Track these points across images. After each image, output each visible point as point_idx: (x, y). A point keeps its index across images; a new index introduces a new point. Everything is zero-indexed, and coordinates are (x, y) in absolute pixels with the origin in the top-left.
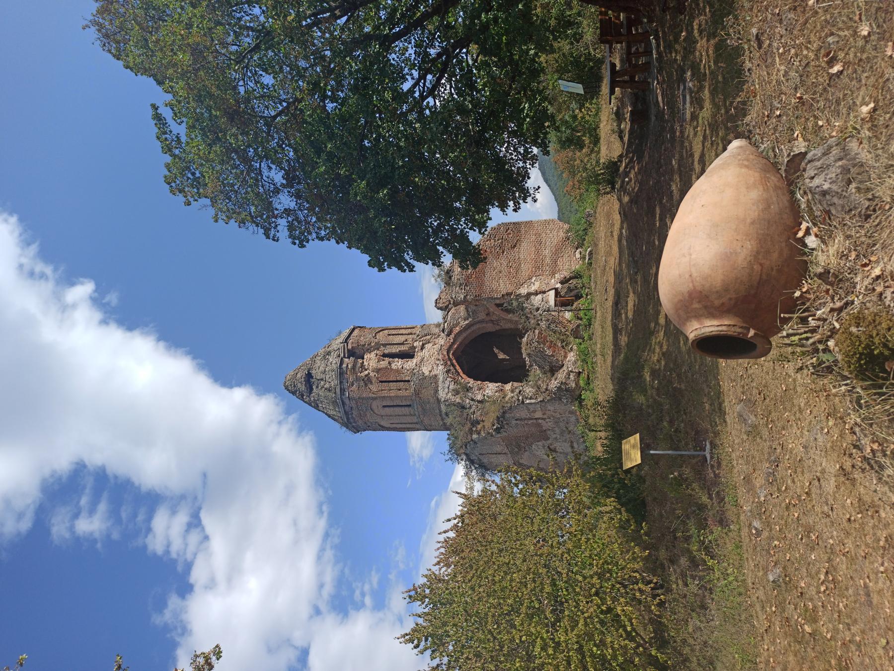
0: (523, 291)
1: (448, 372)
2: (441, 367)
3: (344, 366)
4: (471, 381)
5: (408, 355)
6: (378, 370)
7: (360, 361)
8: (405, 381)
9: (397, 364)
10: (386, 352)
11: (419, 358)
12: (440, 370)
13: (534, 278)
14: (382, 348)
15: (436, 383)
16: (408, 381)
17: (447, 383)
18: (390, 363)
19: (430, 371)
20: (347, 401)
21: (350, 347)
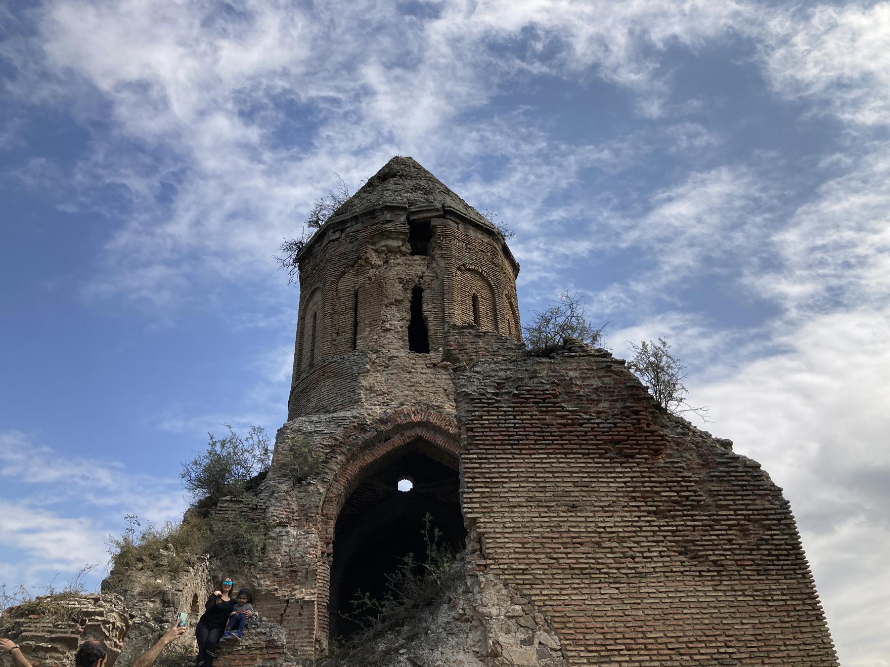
0: (494, 601)
1: (362, 427)
2: (378, 410)
3: (388, 216)
4: (340, 488)
5: (418, 339)
6: (379, 284)
7: (407, 248)
8: (355, 340)
9: (398, 319)
10: (426, 295)
11: (408, 363)
12: (372, 410)
13: (553, 641)
14: (435, 285)
15: (343, 406)
16: (354, 347)
17: (332, 429)
18: (398, 302)
19: (371, 389)
20: (325, 243)
21: (434, 222)
